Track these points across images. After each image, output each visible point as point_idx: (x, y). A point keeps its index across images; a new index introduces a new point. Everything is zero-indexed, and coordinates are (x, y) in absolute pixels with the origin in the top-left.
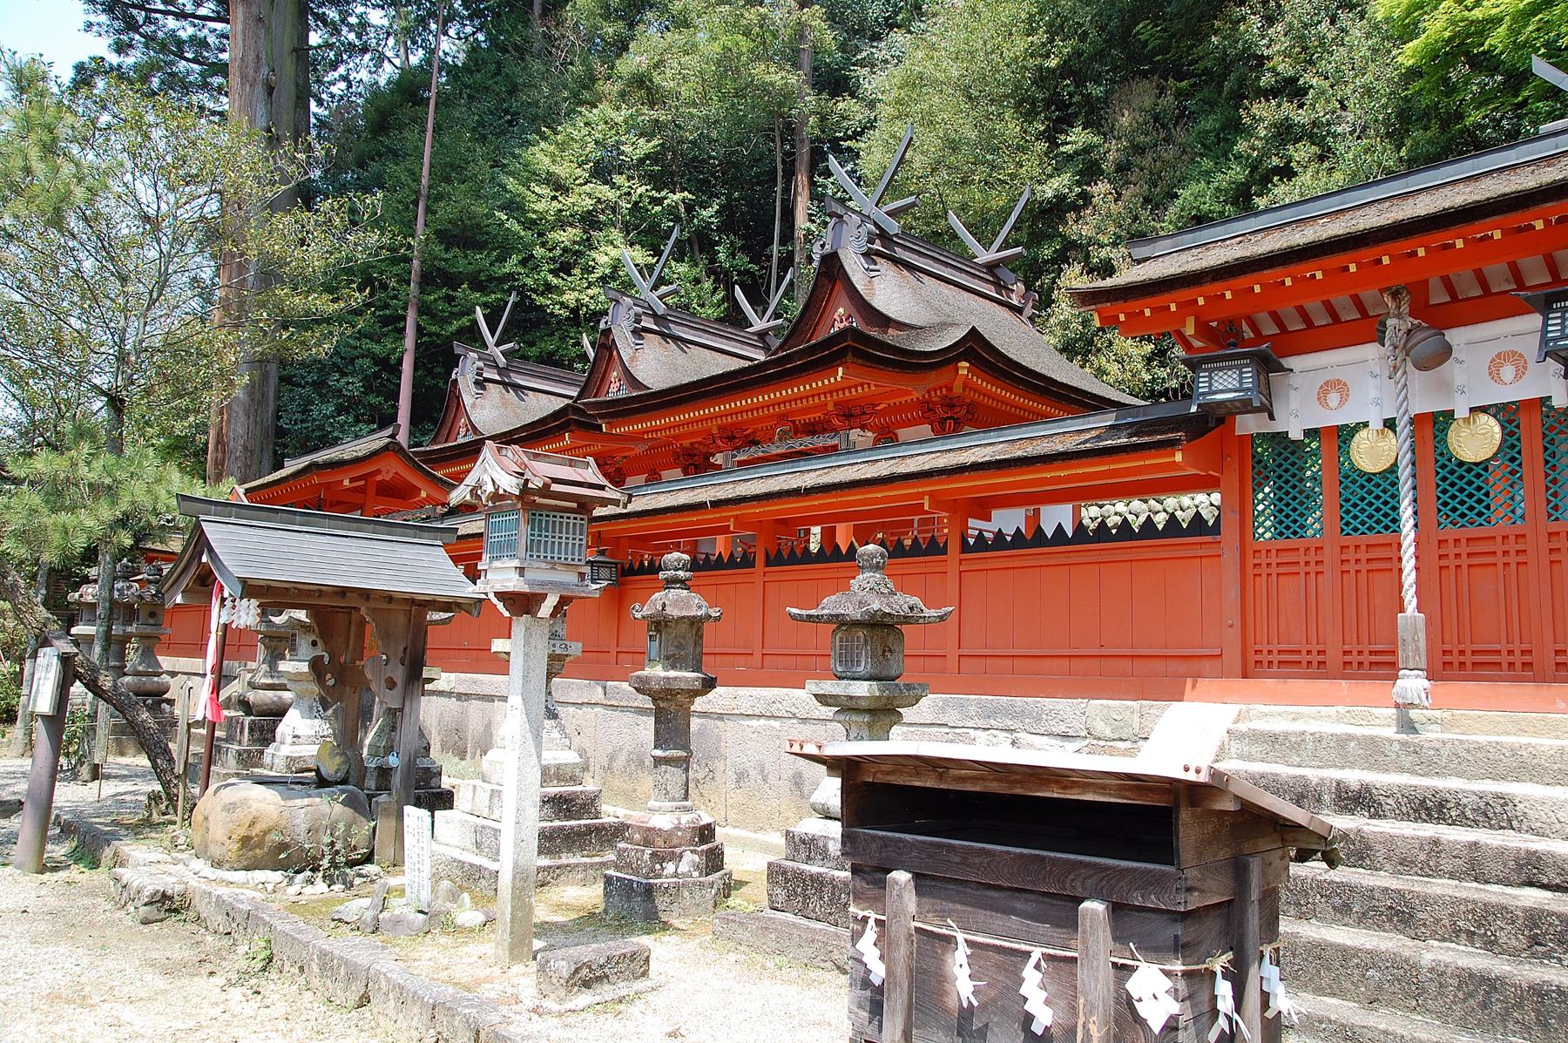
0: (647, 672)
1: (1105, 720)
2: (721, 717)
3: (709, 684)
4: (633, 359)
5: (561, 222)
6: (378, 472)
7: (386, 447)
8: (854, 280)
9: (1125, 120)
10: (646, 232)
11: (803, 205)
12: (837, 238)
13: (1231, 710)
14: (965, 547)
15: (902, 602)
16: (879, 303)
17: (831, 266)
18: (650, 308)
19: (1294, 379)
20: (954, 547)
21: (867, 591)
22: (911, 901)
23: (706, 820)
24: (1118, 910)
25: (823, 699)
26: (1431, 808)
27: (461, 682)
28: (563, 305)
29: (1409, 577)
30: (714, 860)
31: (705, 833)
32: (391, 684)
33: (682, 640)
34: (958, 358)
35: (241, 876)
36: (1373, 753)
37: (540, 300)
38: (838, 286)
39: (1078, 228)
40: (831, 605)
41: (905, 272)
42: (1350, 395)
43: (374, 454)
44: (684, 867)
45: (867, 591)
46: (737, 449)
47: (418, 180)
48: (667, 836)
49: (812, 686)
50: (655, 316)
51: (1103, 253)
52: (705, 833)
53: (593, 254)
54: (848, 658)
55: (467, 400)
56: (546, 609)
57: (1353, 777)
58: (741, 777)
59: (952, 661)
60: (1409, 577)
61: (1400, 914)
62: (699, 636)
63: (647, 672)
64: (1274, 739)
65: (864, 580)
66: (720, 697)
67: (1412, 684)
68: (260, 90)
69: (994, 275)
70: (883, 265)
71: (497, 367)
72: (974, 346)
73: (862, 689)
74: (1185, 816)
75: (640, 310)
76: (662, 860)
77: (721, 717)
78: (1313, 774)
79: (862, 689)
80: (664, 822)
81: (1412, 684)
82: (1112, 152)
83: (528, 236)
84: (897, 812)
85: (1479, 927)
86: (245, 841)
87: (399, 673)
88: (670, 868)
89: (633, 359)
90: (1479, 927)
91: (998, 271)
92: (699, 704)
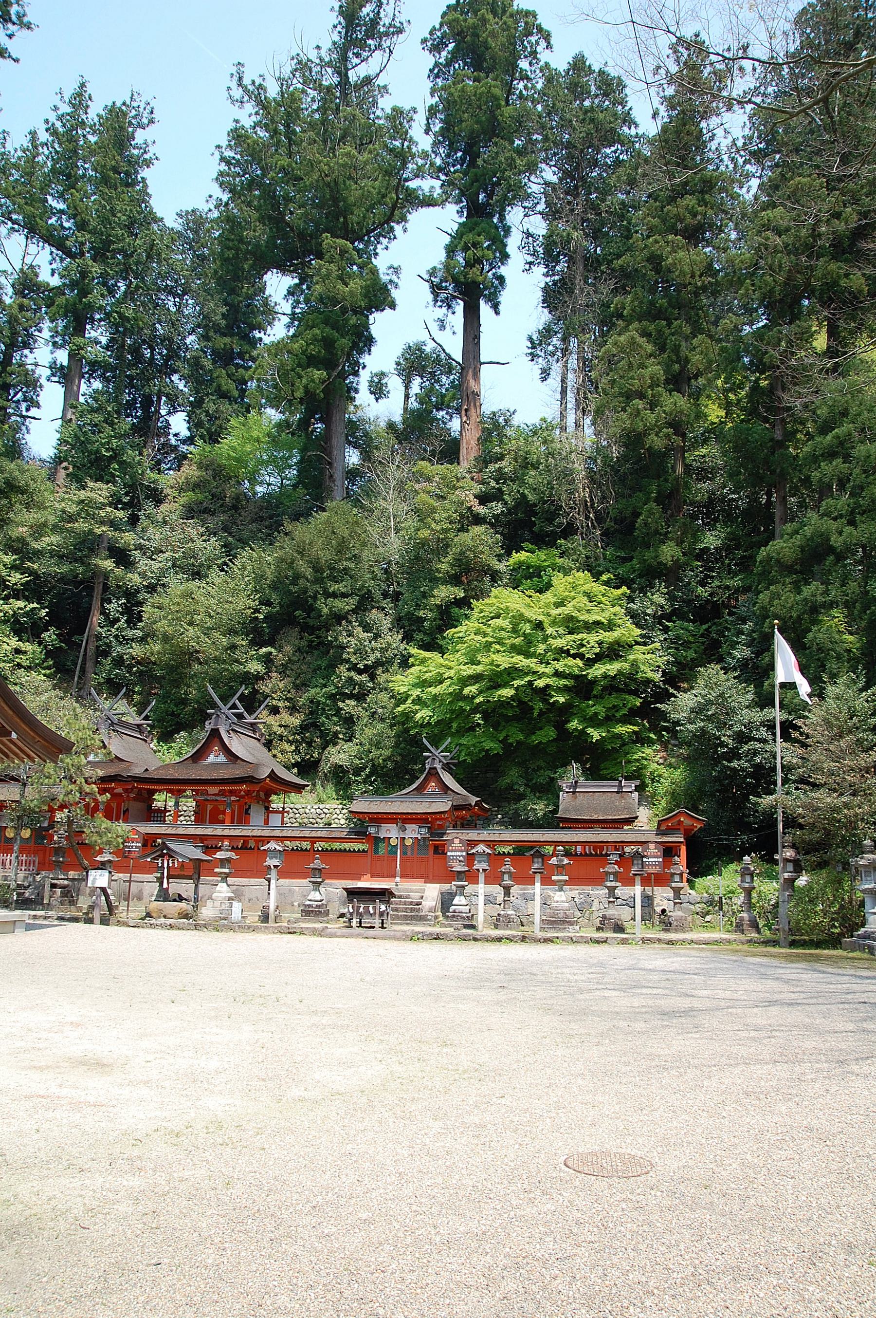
9: (288, 649)
11: (96, 618)
12: (216, 724)
17: (215, 734)
21: (317, 864)
39: (264, 687)
40: (312, 866)
42: (390, 832)
51: (274, 702)
67: (398, 879)
70: (232, 734)
72: (273, 775)
81: (398, 879)
82: (280, 658)
84: (353, 894)
85: (406, 910)
90: (406, 910)
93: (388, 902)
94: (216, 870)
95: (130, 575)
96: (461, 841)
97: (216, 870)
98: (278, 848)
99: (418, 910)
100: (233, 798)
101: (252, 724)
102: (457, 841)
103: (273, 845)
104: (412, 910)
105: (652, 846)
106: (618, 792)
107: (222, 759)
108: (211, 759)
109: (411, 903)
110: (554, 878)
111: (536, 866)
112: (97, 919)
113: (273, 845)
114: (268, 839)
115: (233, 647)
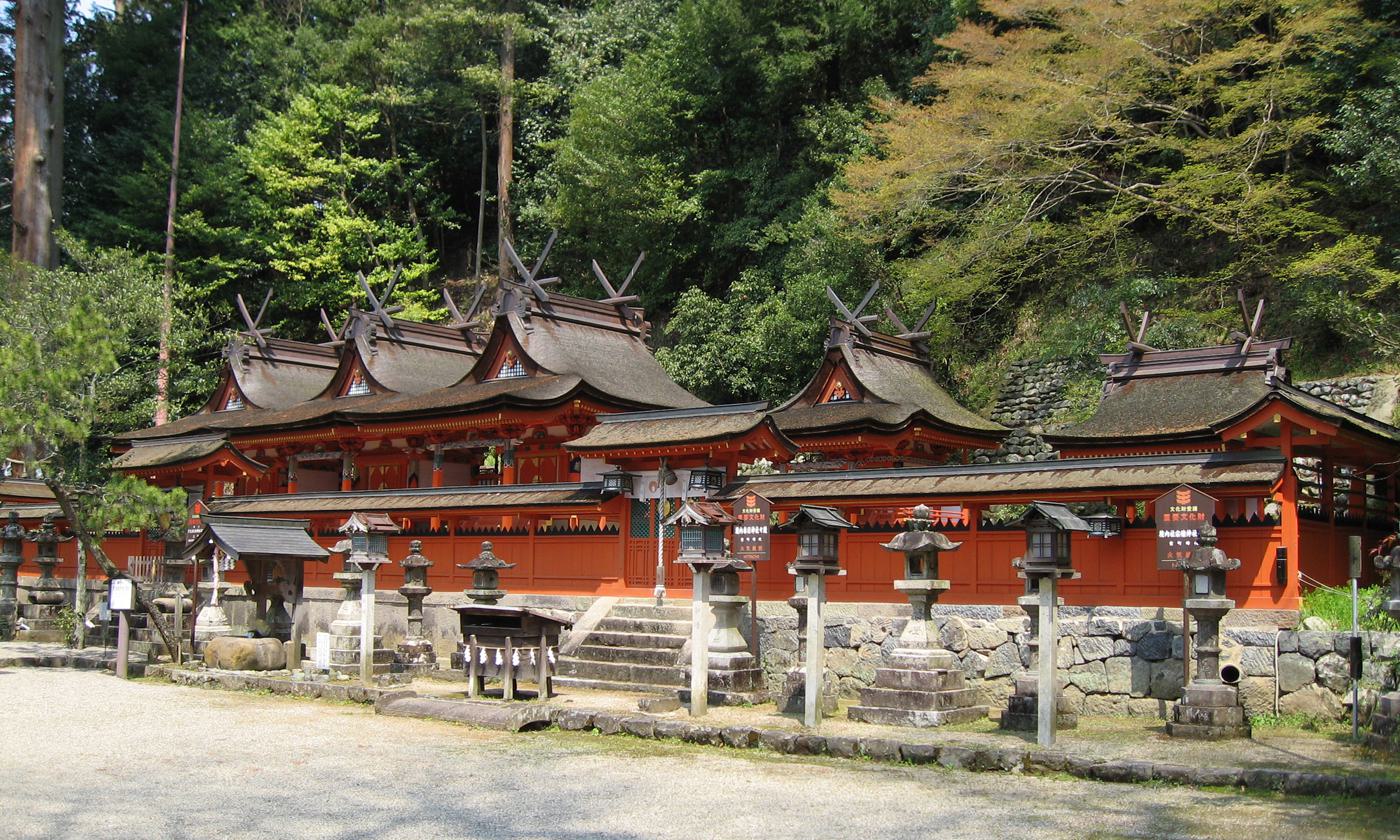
0: (406, 586)
1: (582, 604)
2: (435, 606)
3: (429, 592)
4: (371, 362)
5: (301, 197)
6: (218, 461)
7: (223, 446)
8: (517, 336)
10: (367, 199)
13: (617, 599)
14: (536, 533)
15: (496, 564)
16: (531, 352)
17: (503, 323)
18: (381, 320)
19: (643, 479)
20: (532, 533)
21: (487, 557)
22: (475, 641)
23: (429, 643)
24: (512, 638)
25: (470, 596)
26: (656, 628)
27: (326, 593)
28: (299, 271)
29: (661, 552)
30: (432, 658)
31: (428, 648)
32: (290, 593)
33: (419, 573)
34: (573, 398)
35: (238, 672)
36: (648, 612)
37: (279, 265)
38: (508, 340)
40: (475, 563)
41: (552, 325)
43: (217, 450)
44: (421, 660)
45: (486, 556)
46: (445, 442)
47: (168, 158)
48: (414, 648)
49: (466, 592)
50: (385, 326)
52: (428, 648)
53: (323, 223)
54: (478, 581)
55: (238, 375)
56: (374, 568)
57: (638, 620)
58: (444, 633)
59: (530, 581)
60: (661, 552)
61: (633, 657)
62: (425, 572)
63: (406, 586)
64: (624, 609)
65: (484, 554)
66: (435, 597)
68: (42, 99)
69: (620, 312)
71: (258, 345)
73: (481, 592)
74: (523, 618)
75: (373, 325)
76: (413, 657)
77: (435, 606)
78: (628, 620)
79: (481, 592)
80: (412, 643)
81: (660, 588)
83: (266, 210)
86: (239, 658)
87: (293, 588)
88: (416, 660)
89: (371, 362)
91: (622, 309)
92: (425, 600)
93: (553, 641)
94: (337, 576)
95: (535, 87)
96: (759, 501)
97: (337, 576)
98: (363, 528)
99: (671, 660)
100: (514, 442)
101: (618, 306)
102: (751, 501)
103: (356, 523)
104: (661, 658)
105: (1183, 497)
106: (1226, 372)
107: (520, 370)
108: (504, 374)
109: (667, 644)
110: (899, 584)
111: (804, 553)
112: (122, 668)
113: (356, 523)
114: (346, 514)
115: (640, 175)
